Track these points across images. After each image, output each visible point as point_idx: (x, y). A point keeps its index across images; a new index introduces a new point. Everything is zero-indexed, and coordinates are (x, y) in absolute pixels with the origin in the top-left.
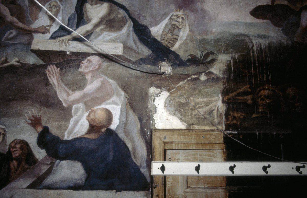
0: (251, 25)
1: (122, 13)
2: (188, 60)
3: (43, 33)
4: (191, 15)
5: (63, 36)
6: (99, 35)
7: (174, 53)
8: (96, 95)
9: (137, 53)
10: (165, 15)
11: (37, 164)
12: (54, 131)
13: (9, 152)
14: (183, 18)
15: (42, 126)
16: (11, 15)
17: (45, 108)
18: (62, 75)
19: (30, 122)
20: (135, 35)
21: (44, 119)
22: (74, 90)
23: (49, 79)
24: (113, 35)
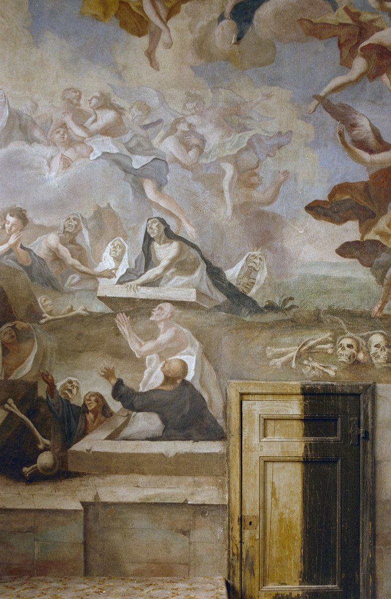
0: (335, 265)
1: (193, 252)
2: (266, 307)
3: (109, 277)
4: (269, 254)
5: (132, 280)
6: (170, 280)
7: (250, 298)
8: (170, 346)
9: (211, 299)
10: (241, 256)
11: (113, 416)
12: (128, 382)
13: (84, 404)
14: (260, 259)
15: (115, 378)
16: (72, 257)
17: (118, 360)
18: (133, 324)
19: (103, 374)
20: (208, 279)
21: (117, 371)
22: (146, 341)
23: (120, 328)
24: (186, 279)
